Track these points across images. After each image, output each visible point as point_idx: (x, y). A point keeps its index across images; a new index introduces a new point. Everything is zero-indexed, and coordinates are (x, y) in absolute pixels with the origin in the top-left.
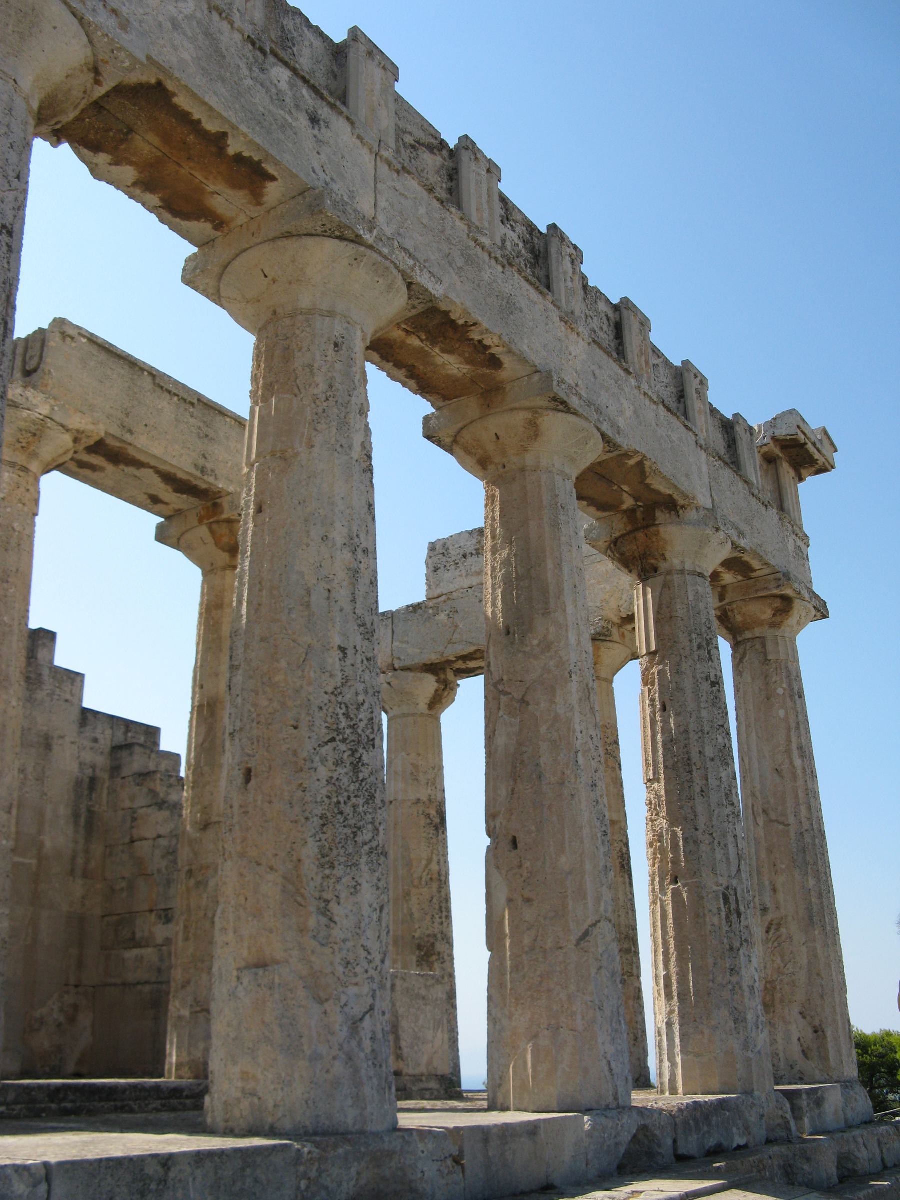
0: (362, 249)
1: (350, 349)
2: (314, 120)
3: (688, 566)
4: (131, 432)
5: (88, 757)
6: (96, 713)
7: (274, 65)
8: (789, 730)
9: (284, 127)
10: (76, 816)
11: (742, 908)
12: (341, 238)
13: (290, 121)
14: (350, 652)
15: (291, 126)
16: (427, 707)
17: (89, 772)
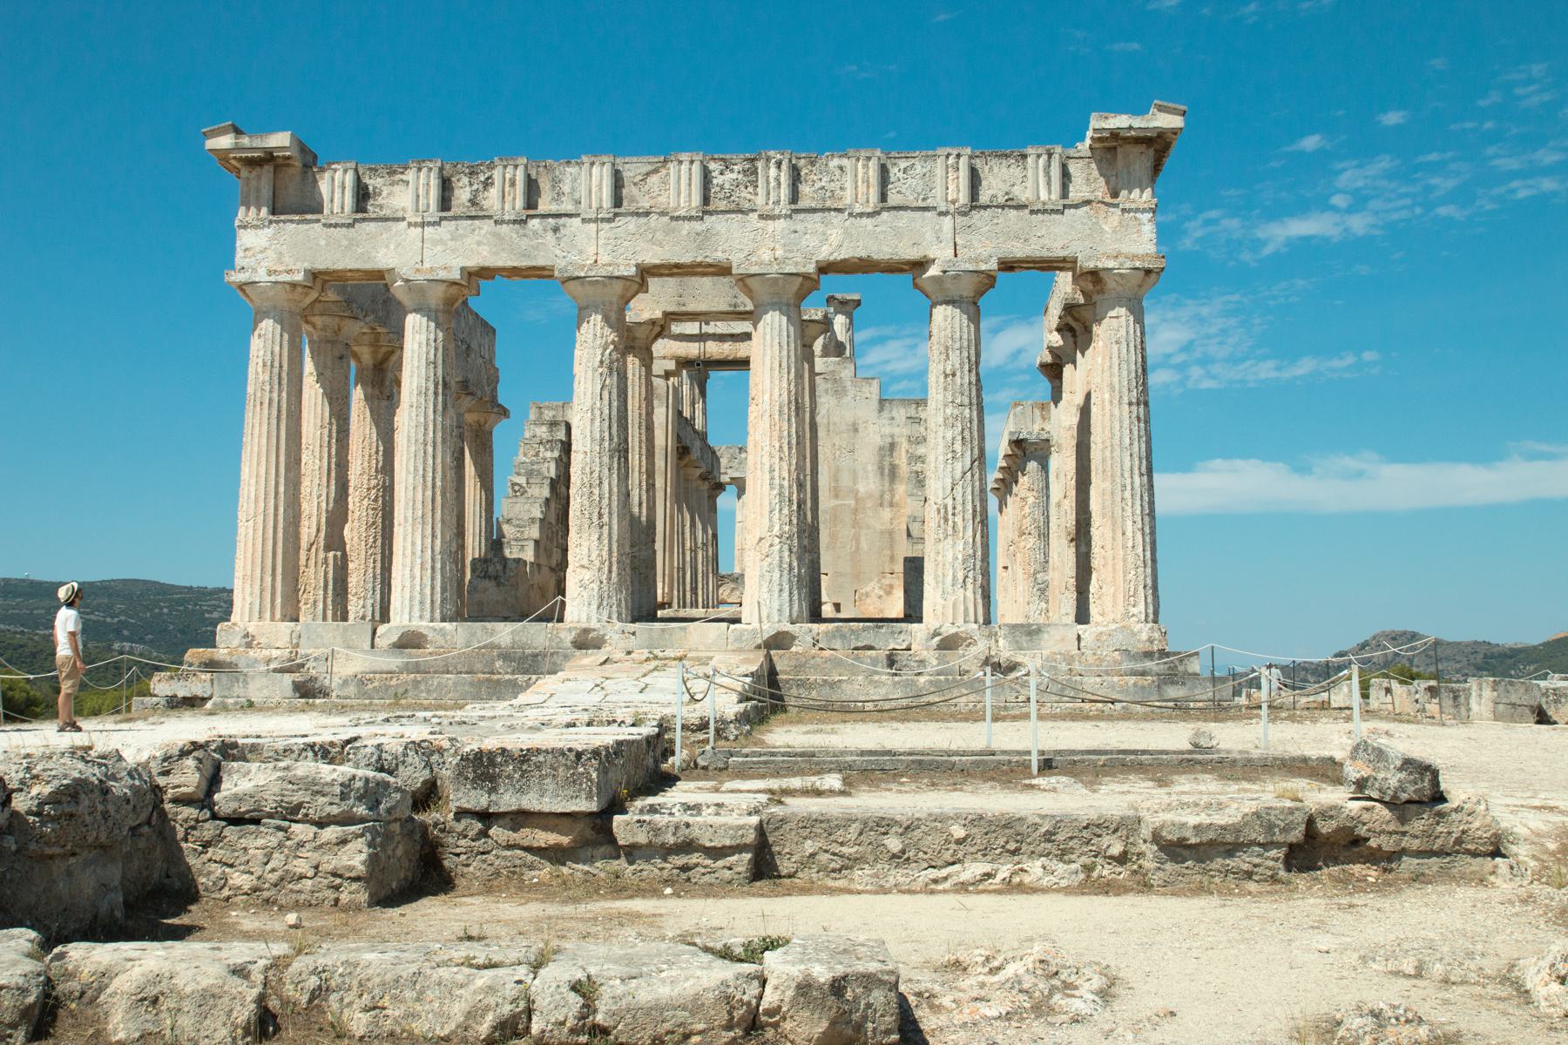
2: (556, 230)
5: (887, 430)
9: (536, 248)
10: (881, 468)
11: (950, 517)
17: (890, 440)
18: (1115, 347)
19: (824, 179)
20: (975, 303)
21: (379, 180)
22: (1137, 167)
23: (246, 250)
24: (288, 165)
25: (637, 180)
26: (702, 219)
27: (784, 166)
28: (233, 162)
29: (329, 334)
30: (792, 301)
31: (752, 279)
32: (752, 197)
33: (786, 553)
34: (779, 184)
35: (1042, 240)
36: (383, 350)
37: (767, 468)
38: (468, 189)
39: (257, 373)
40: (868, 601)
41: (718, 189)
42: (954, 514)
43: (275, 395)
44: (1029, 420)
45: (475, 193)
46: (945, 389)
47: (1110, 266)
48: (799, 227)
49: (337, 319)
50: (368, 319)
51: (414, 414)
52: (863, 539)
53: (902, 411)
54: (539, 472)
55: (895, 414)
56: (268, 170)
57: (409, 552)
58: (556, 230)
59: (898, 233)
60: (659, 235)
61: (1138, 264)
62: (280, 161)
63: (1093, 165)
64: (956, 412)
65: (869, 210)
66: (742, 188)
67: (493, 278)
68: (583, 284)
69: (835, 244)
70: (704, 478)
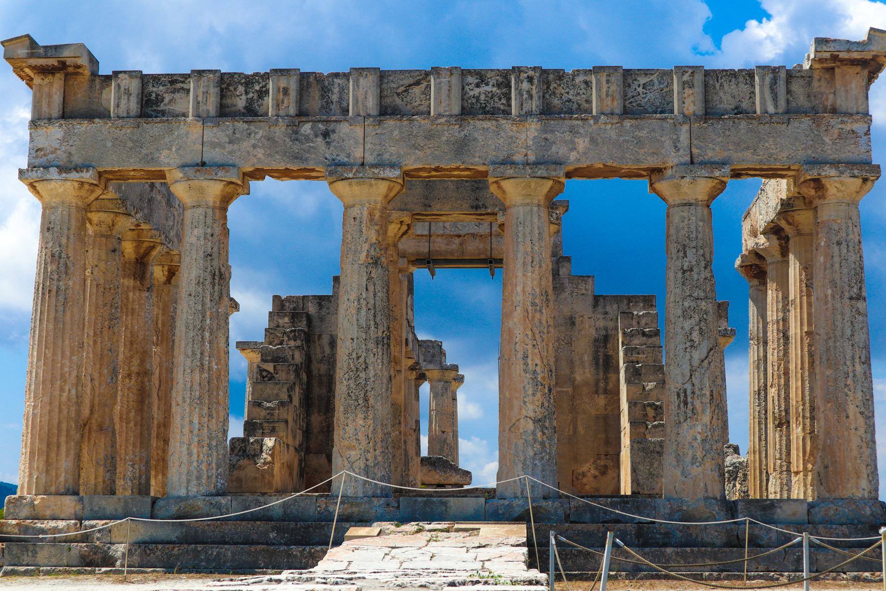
0: (350, 180)
1: (361, 218)
2: (326, 135)
3: (678, 202)
4: (430, 206)
5: (601, 323)
6: (604, 297)
7: (303, 125)
8: (825, 269)
10: (596, 359)
11: (689, 400)
12: (342, 180)
13: (311, 144)
14: (355, 340)
15: (313, 147)
16: (780, 256)
17: (604, 332)
18: (836, 249)
19: (571, 92)
20: (708, 206)
21: (161, 88)
22: (853, 85)
23: (37, 151)
24: (77, 74)
25: (400, 91)
27: (536, 81)
28: (27, 70)
29: (104, 228)
30: (542, 202)
31: (506, 181)
32: (506, 108)
33: (539, 434)
36: (146, 245)
37: (520, 355)
38: (244, 97)
39: (46, 264)
40: (585, 480)
41: (474, 101)
42: (693, 398)
45: (250, 102)
46: (683, 284)
48: (549, 136)
49: (112, 215)
50: (138, 216)
51: (191, 303)
52: (579, 424)
53: (615, 306)
54: (285, 360)
55: (608, 309)
56: (59, 76)
57: (186, 430)
58: (326, 135)
59: (639, 142)
60: (421, 141)
62: (71, 70)
64: (693, 304)
65: (615, 121)
66: (496, 99)
67: (263, 178)
68: (350, 184)
70: (412, 369)
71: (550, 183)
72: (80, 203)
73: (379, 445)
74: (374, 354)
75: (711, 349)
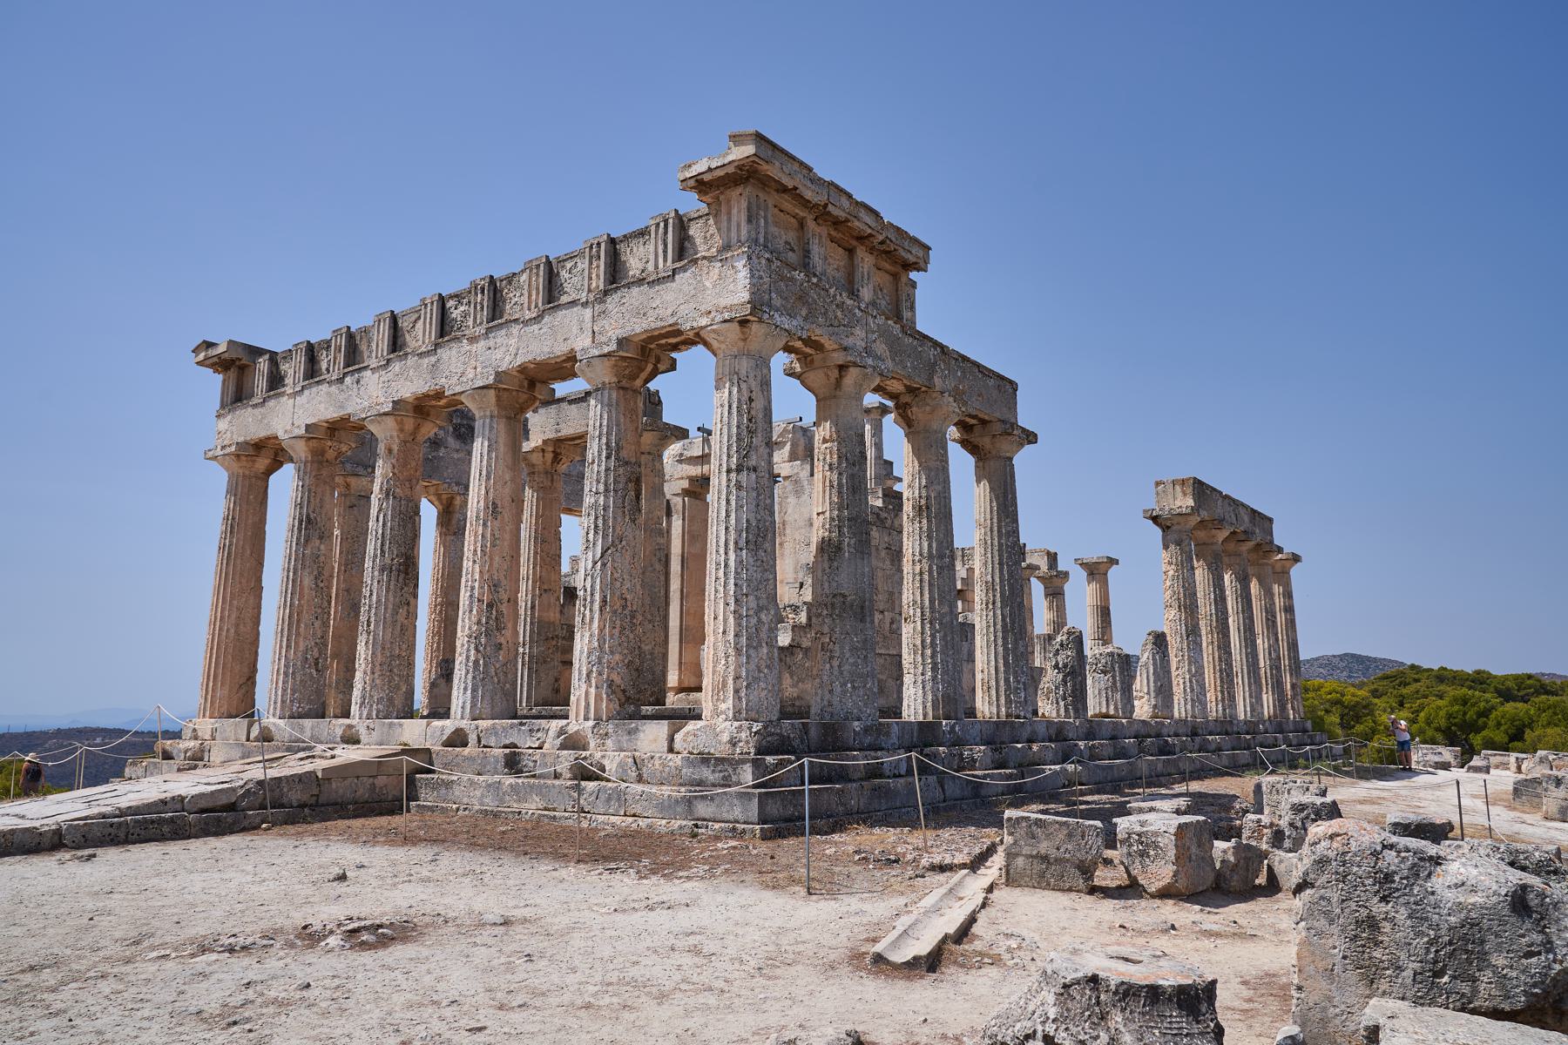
26: (435, 350)
33: (473, 652)
34: (482, 308)
35: (657, 311)
43: (227, 541)
44: (1170, 497)
47: (704, 324)
58: (358, 382)
61: (726, 316)
62: (237, 363)
63: (711, 222)
69: (514, 351)
71: (492, 391)
72: (247, 473)
73: (378, 668)
74: (379, 582)
75: (609, 548)
